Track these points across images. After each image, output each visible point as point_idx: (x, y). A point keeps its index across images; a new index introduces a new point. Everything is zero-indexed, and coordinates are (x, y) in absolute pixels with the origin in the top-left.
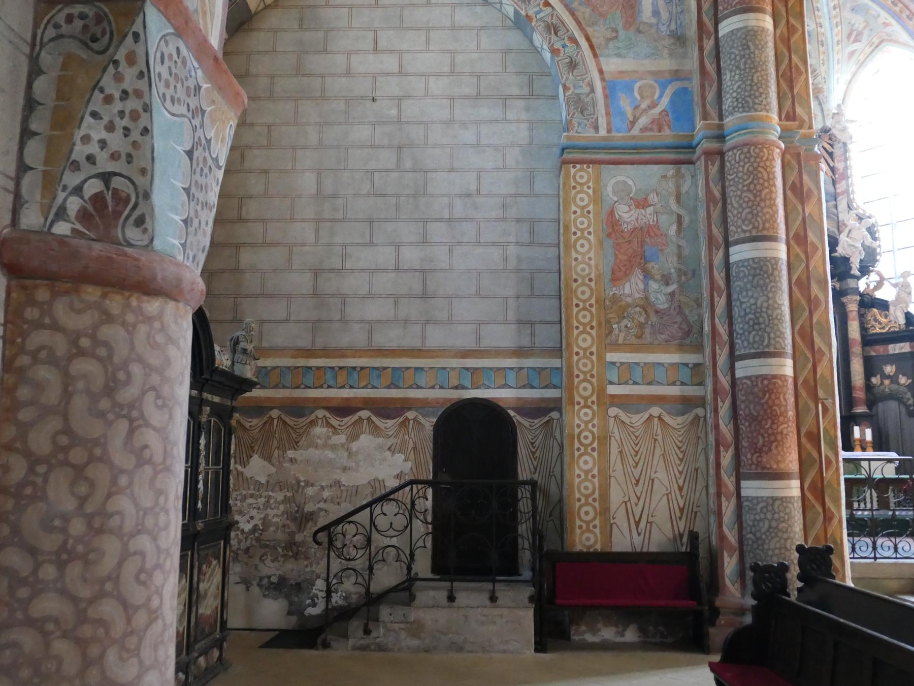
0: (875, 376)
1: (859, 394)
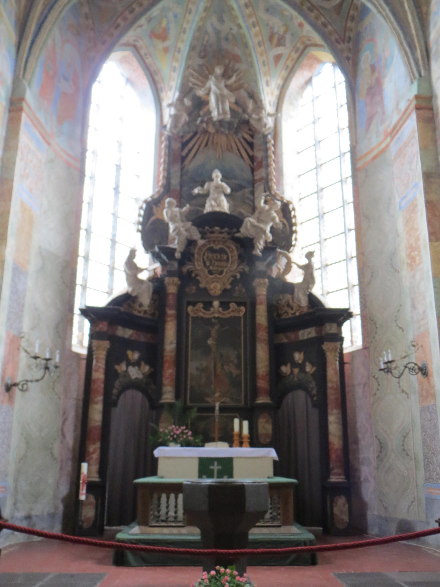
0: (286, 364)
1: (262, 384)
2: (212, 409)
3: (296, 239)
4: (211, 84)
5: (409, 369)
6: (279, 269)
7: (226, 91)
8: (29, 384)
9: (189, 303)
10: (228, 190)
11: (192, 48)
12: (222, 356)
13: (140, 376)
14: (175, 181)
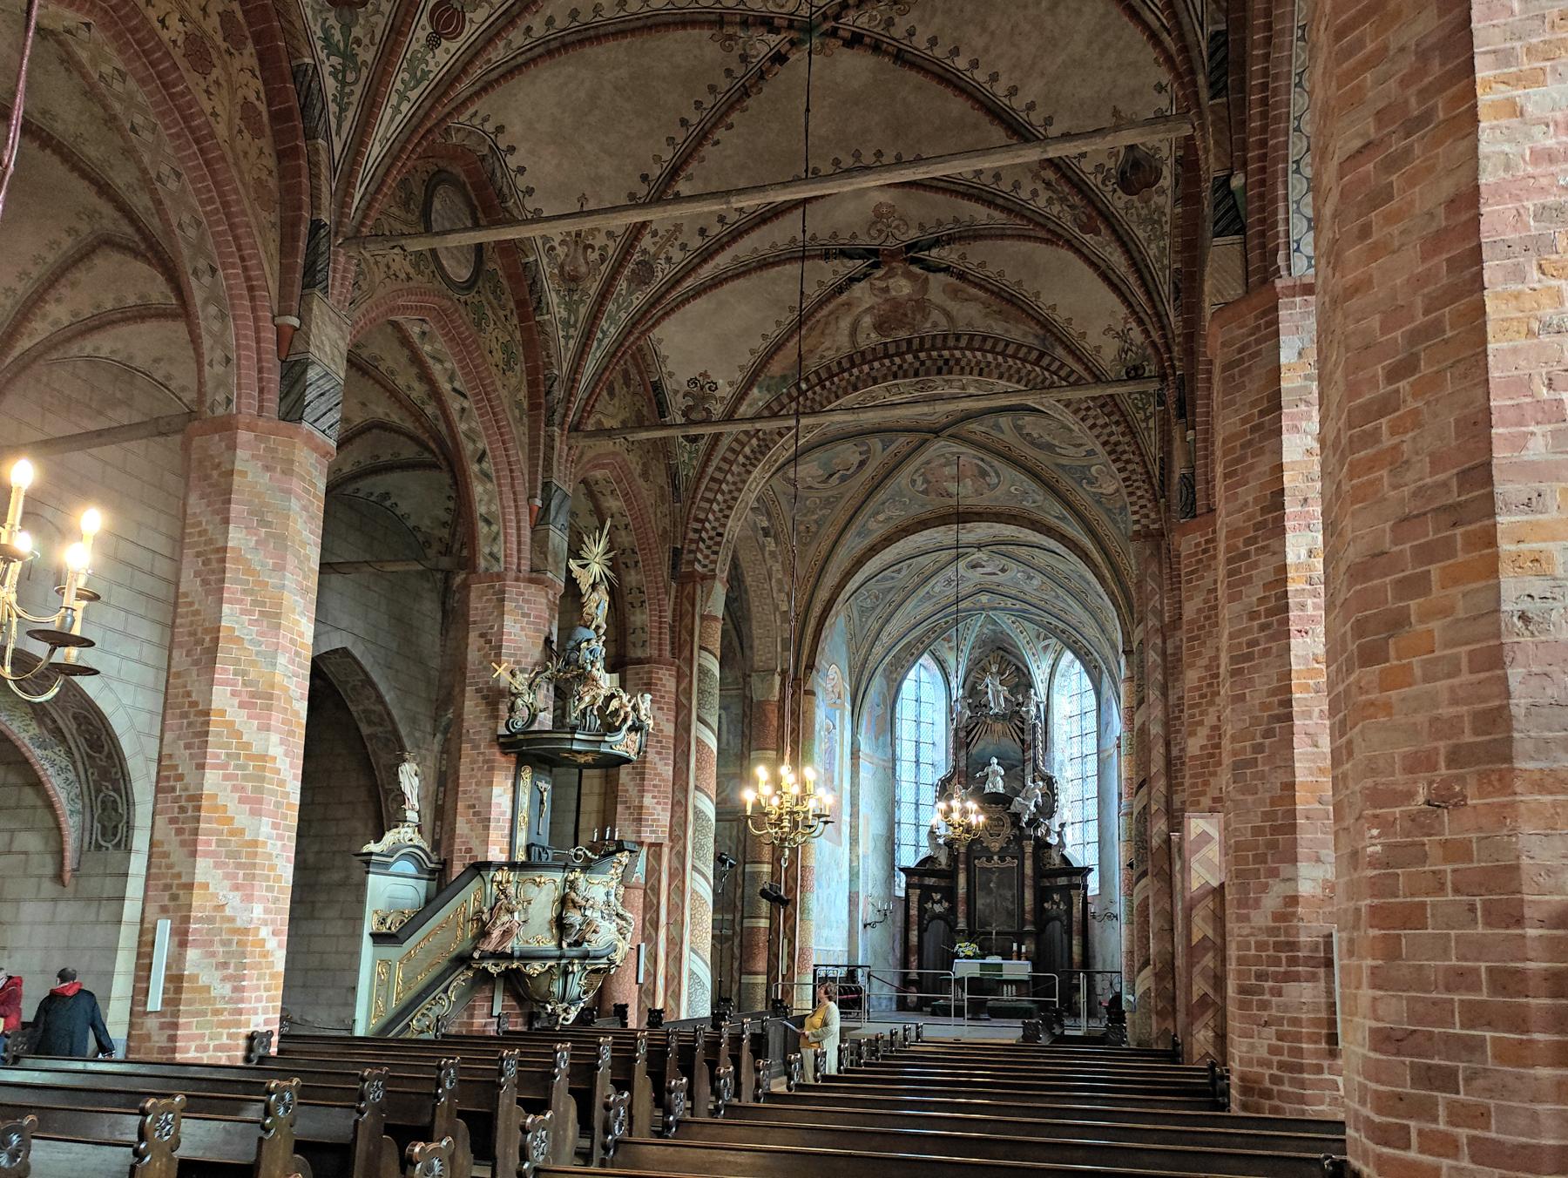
1: (1028, 916)
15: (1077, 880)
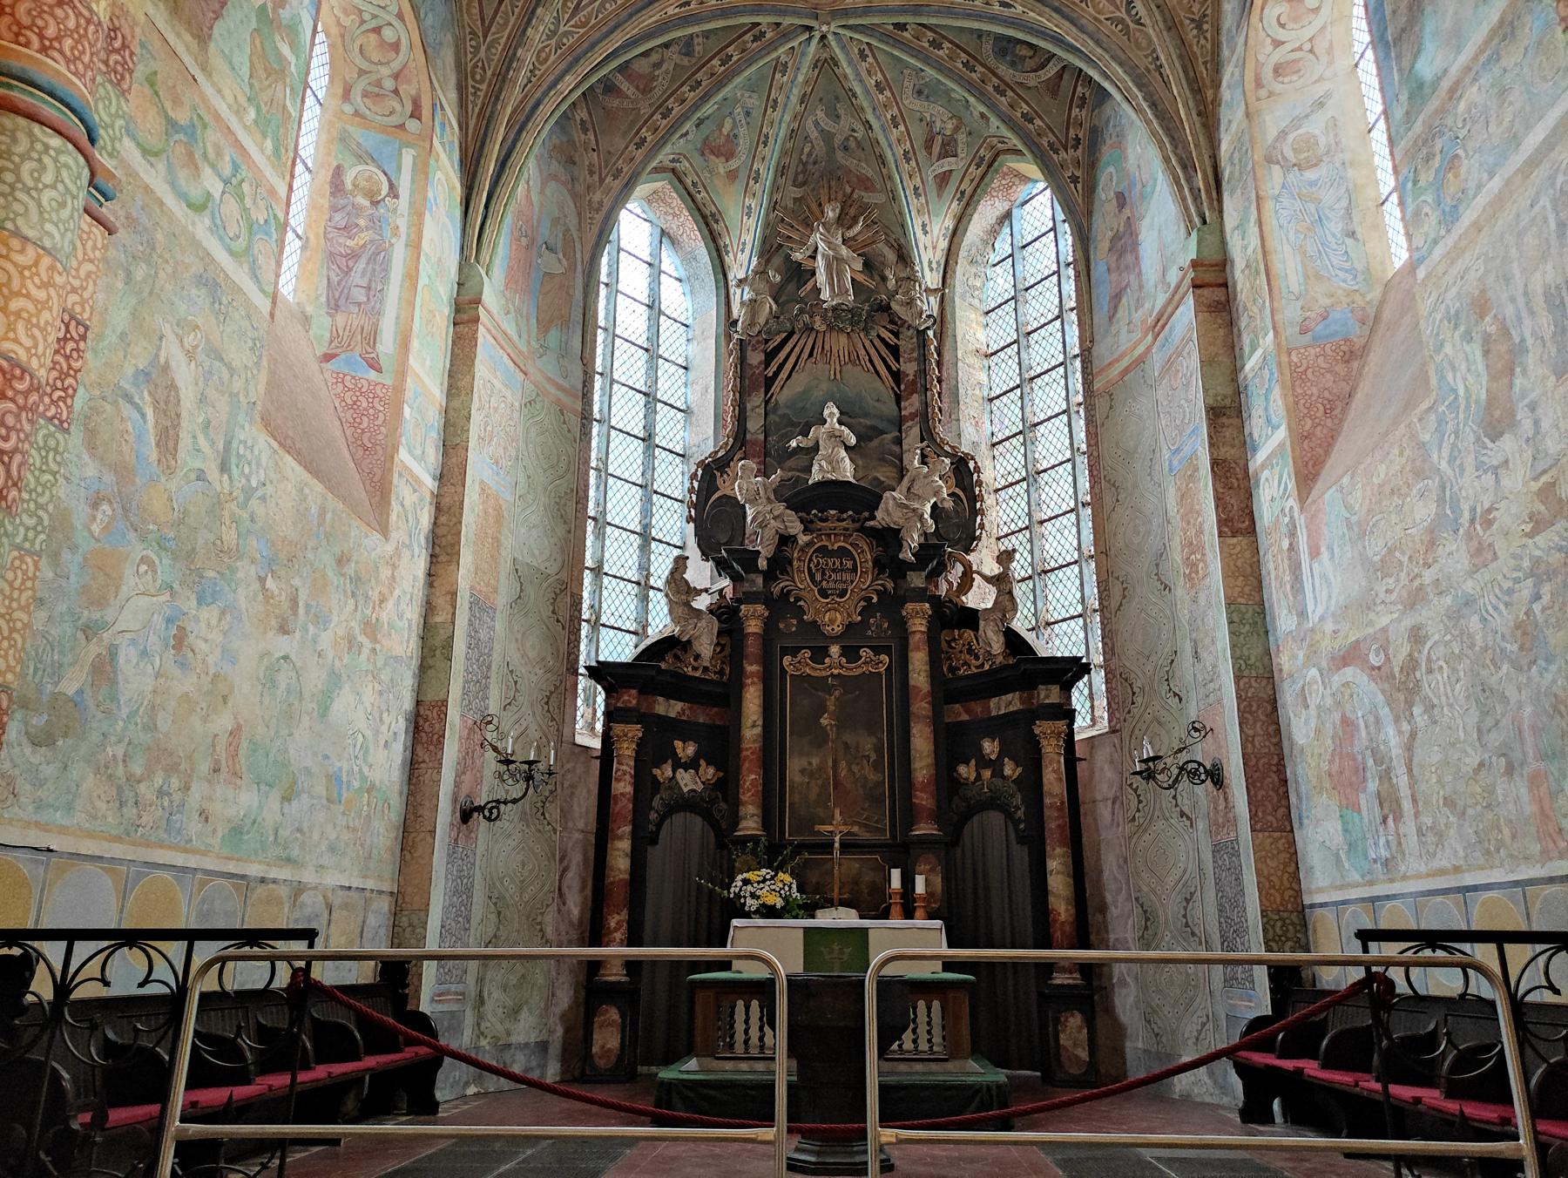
1: (923, 799)
2: (829, 846)
3: (982, 526)
4: (817, 238)
5: (1189, 773)
6: (951, 584)
7: (844, 251)
8: (502, 807)
9: (785, 651)
10: (853, 441)
11: (781, 171)
12: (847, 746)
13: (699, 787)
14: (754, 425)
15: (1049, 694)
